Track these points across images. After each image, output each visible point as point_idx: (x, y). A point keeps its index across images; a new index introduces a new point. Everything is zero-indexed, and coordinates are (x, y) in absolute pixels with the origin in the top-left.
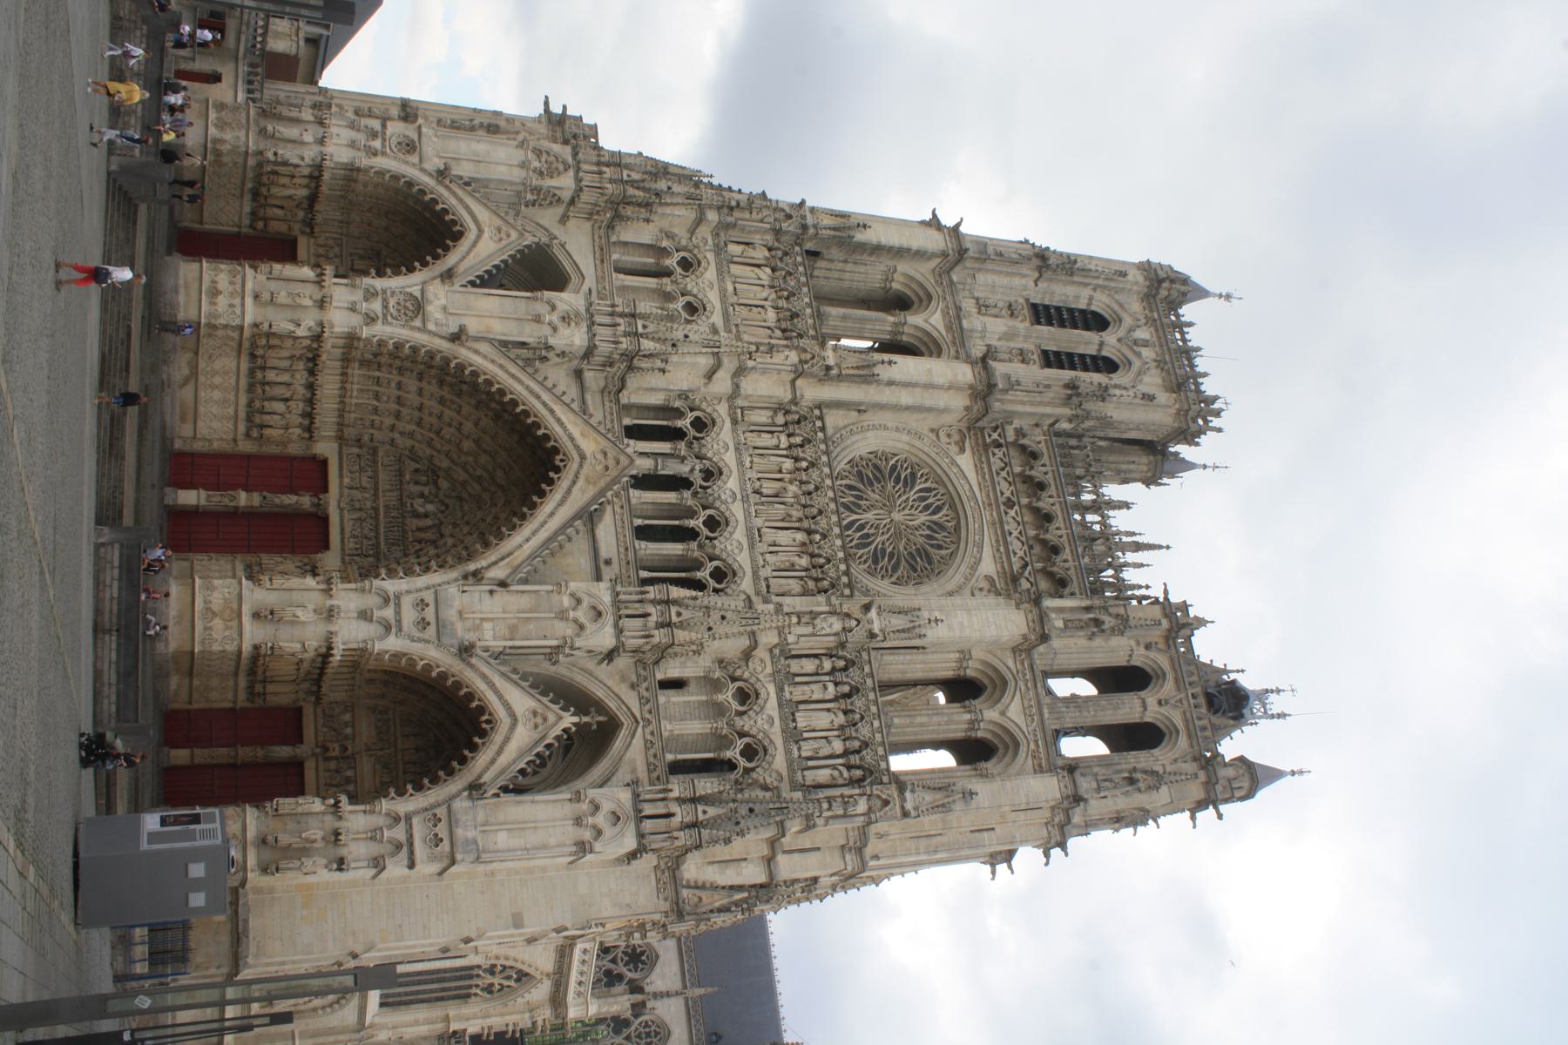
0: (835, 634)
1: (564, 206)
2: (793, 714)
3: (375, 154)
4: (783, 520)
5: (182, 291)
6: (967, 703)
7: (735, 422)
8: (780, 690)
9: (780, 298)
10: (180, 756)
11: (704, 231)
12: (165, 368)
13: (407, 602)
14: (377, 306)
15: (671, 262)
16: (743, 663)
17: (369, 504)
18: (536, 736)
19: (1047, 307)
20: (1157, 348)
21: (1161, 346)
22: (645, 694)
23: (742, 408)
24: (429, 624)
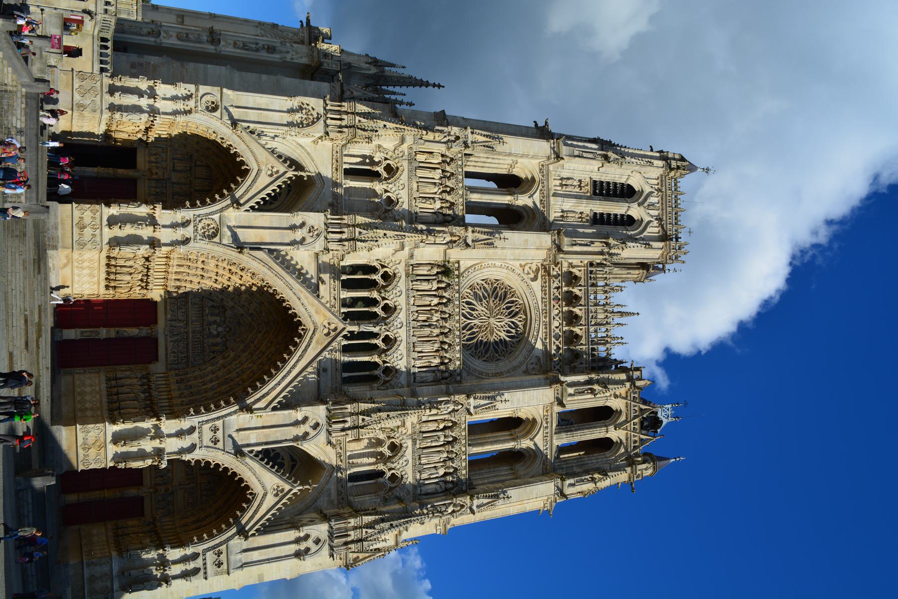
0: (450, 413)
1: (315, 138)
2: (420, 456)
3: (190, 112)
4: (428, 337)
5: (60, 227)
6: (513, 431)
7: (407, 275)
8: (414, 442)
9: (444, 192)
10: (72, 498)
11: (405, 147)
12: (50, 260)
13: (206, 427)
14: (189, 232)
15: (380, 169)
16: (396, 430)
17: (182, 330)
18: (277, 499)
19: (602, 182)
20: (660, 211)
21: (662, 209)
22: (340, 451)
23: (412, 265)
24: (218, 441)
